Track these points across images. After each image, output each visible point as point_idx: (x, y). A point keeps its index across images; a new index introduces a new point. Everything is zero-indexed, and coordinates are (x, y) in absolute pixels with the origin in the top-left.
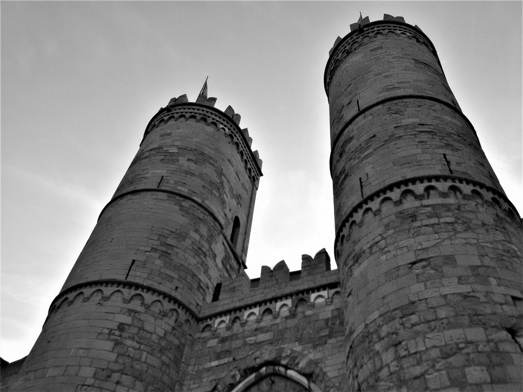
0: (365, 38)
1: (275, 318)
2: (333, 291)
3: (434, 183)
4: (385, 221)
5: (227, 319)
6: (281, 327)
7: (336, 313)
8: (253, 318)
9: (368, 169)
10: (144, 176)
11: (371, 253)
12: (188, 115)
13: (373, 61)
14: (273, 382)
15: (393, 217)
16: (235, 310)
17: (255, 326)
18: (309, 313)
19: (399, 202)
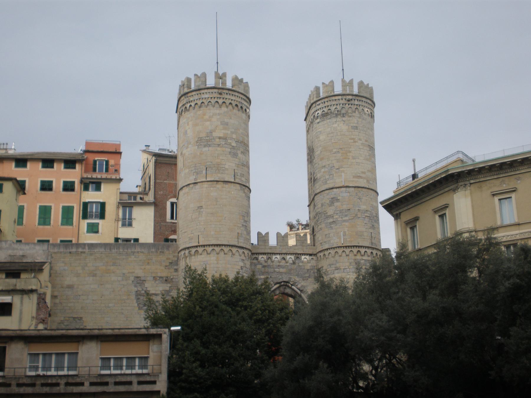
0: (350, 109)
1: (287, 262)
2: (311, 257)
3: (367, 250)
4: (350, 261)
5: (265, 257)
6: (289, 268)
7: (311, 268)
8: (276, 259)
9: (346, 229)
10: (223, 166)
11: (344, 272)
12: (234, 103)
13: (352, 141)
14: (285, 288)
15: (353, 261)
16: (268, 253)
17: (278, 264)
18: (301, 264)
19: (355, 255)
